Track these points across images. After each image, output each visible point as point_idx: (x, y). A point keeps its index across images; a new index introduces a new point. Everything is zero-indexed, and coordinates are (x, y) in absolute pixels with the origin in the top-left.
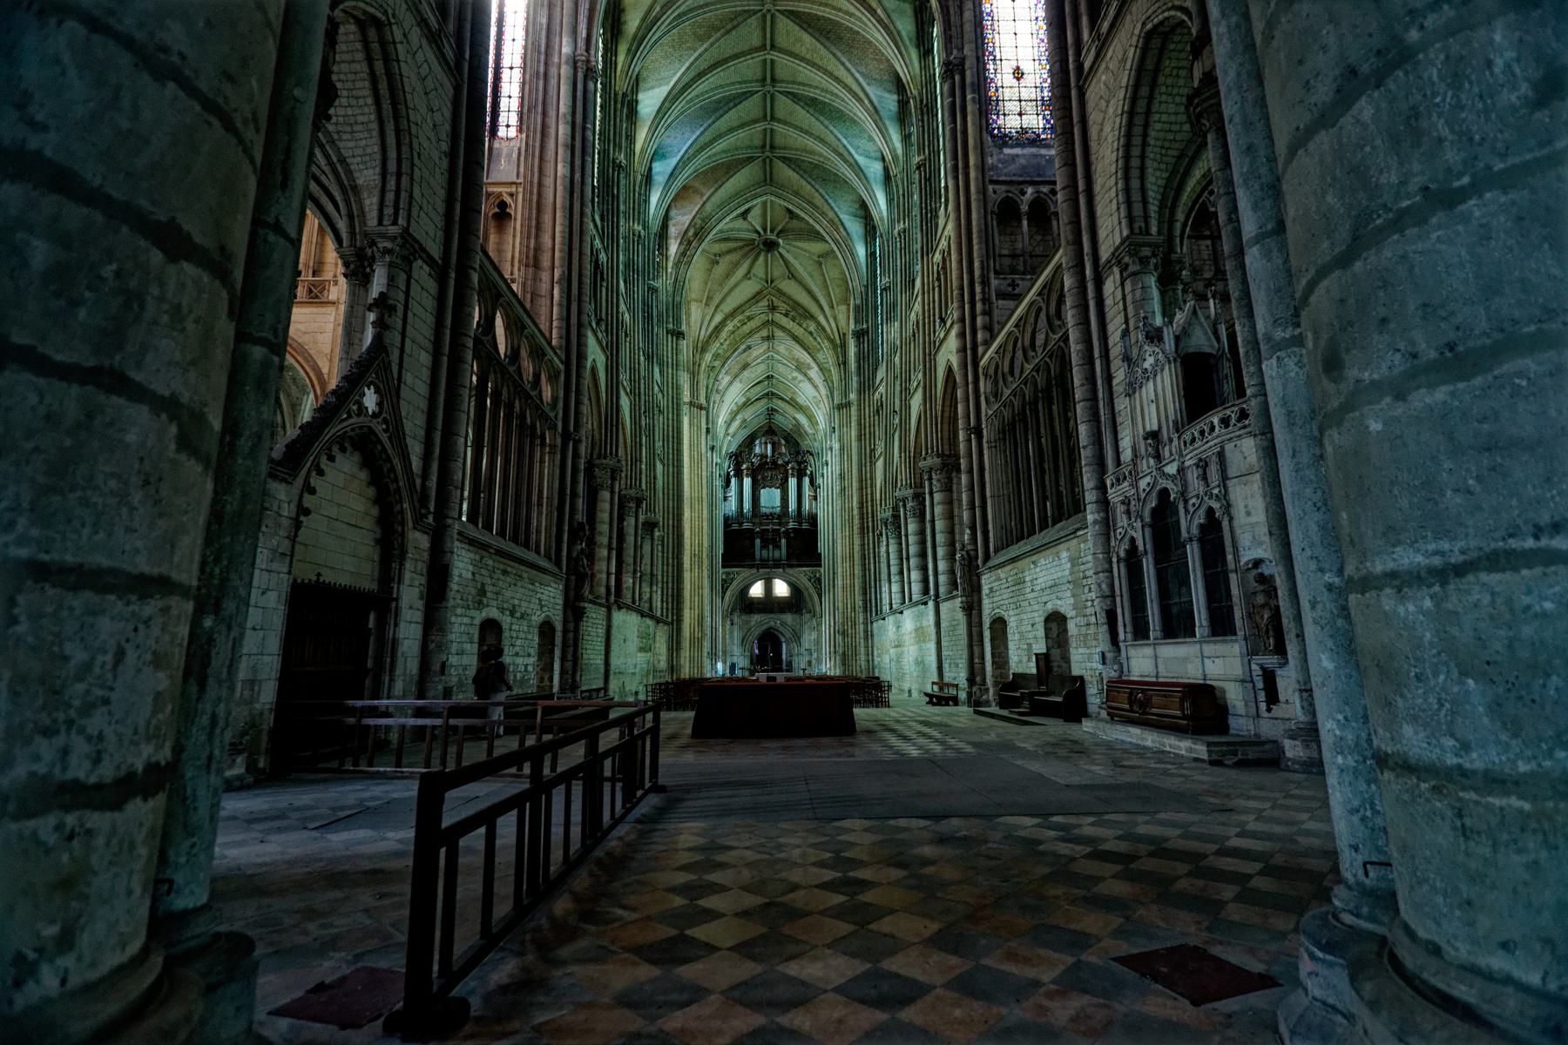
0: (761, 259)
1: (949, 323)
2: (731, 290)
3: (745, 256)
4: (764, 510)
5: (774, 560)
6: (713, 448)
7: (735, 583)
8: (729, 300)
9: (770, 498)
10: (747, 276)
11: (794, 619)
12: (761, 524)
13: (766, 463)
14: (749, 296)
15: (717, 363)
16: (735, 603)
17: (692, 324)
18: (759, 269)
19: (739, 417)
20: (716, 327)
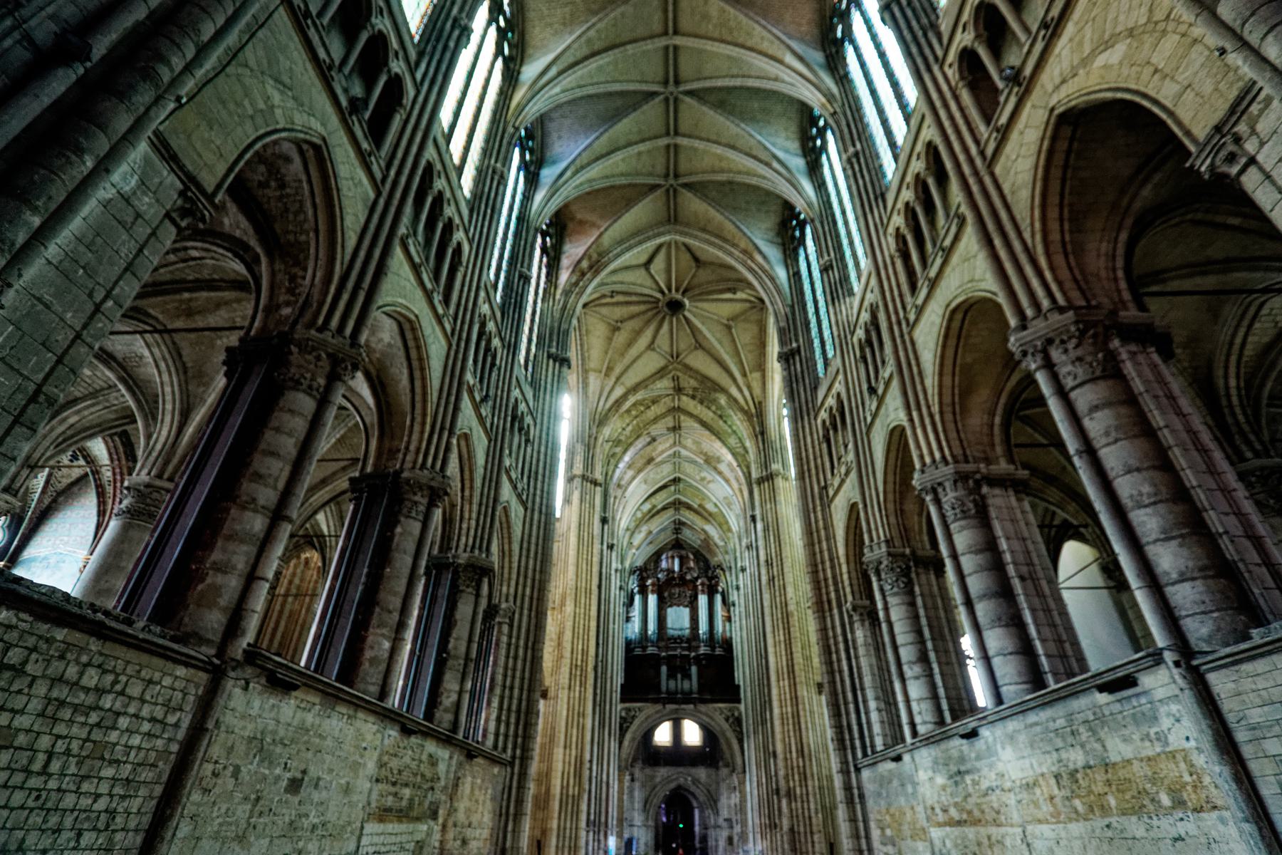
0: (666, 327)
1: (880, 391)
2: (634, 361)
3: (648, 322)
4: (671, 632)
5: (683, 692)
6: (611, 547)
7: (637, 722)
8: (631, 373)
9: (678, 618)
10: (651, 346)
11: (709, 776)
12: (667, 648)
13: (674, 578)
14: (653, 371)
15: (618, 450)
16: (638, 749)
17: (590, 394)
18: (663, 341)
19: (644, 529)
20: (617, 401)
